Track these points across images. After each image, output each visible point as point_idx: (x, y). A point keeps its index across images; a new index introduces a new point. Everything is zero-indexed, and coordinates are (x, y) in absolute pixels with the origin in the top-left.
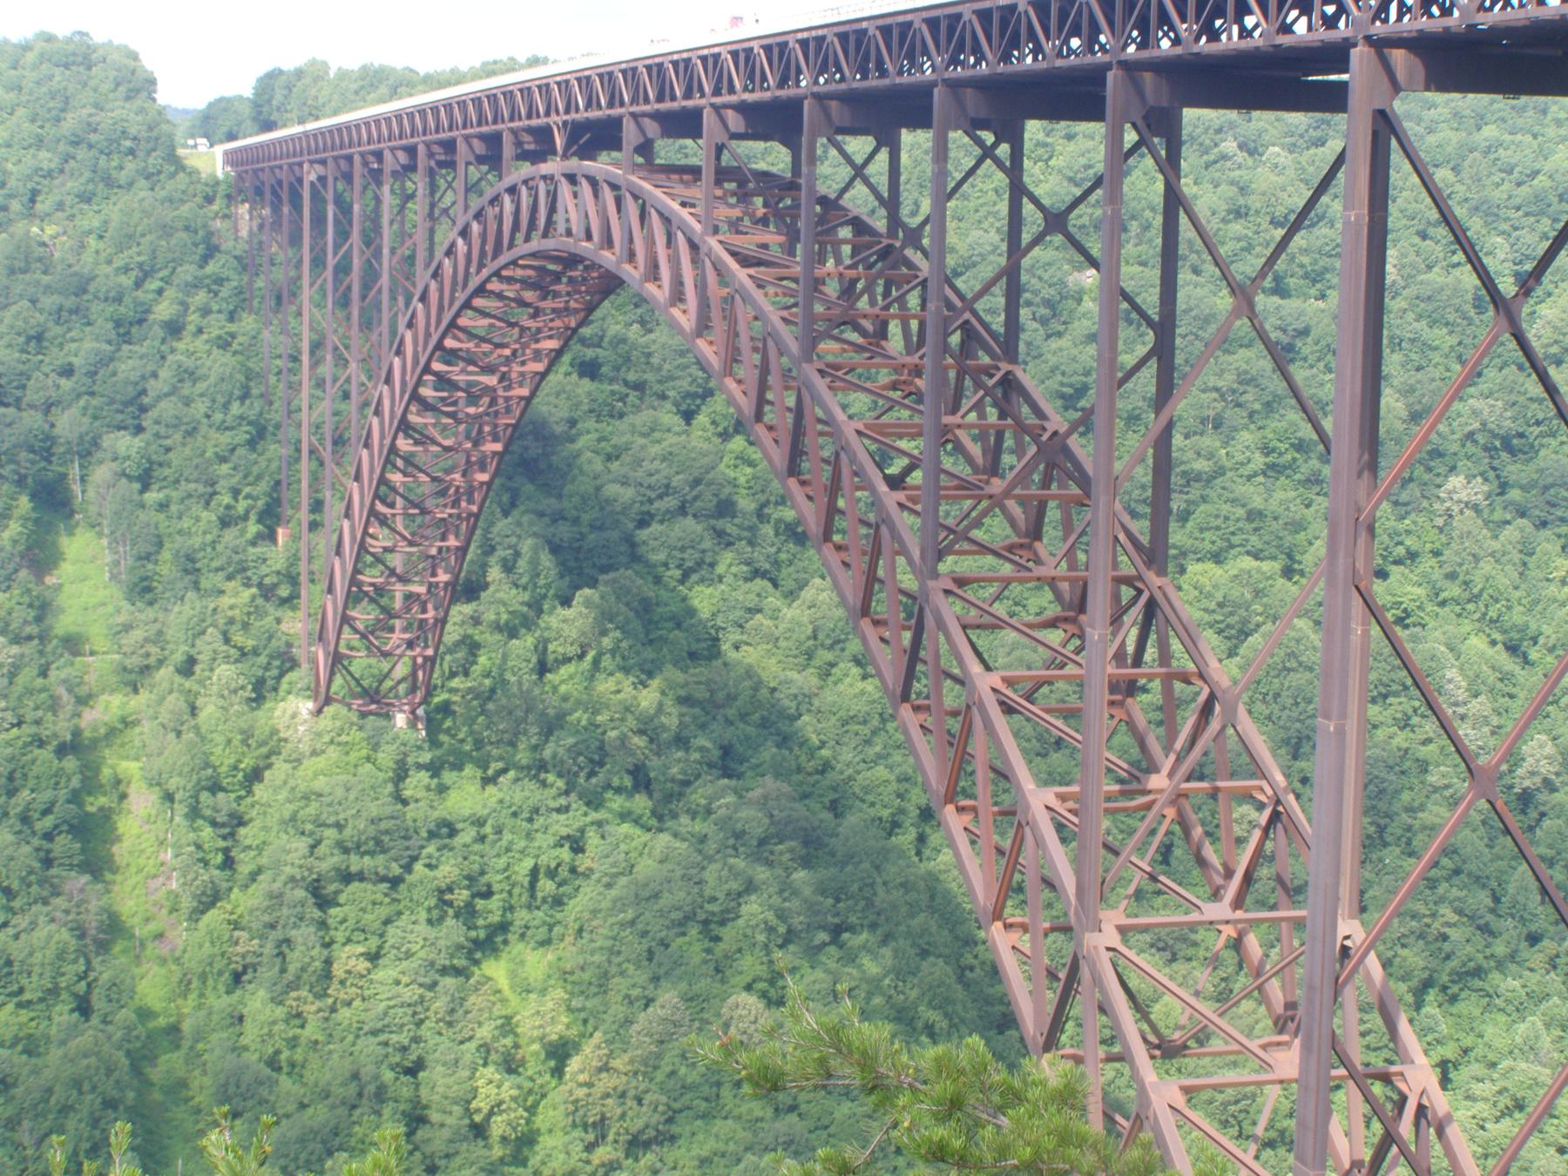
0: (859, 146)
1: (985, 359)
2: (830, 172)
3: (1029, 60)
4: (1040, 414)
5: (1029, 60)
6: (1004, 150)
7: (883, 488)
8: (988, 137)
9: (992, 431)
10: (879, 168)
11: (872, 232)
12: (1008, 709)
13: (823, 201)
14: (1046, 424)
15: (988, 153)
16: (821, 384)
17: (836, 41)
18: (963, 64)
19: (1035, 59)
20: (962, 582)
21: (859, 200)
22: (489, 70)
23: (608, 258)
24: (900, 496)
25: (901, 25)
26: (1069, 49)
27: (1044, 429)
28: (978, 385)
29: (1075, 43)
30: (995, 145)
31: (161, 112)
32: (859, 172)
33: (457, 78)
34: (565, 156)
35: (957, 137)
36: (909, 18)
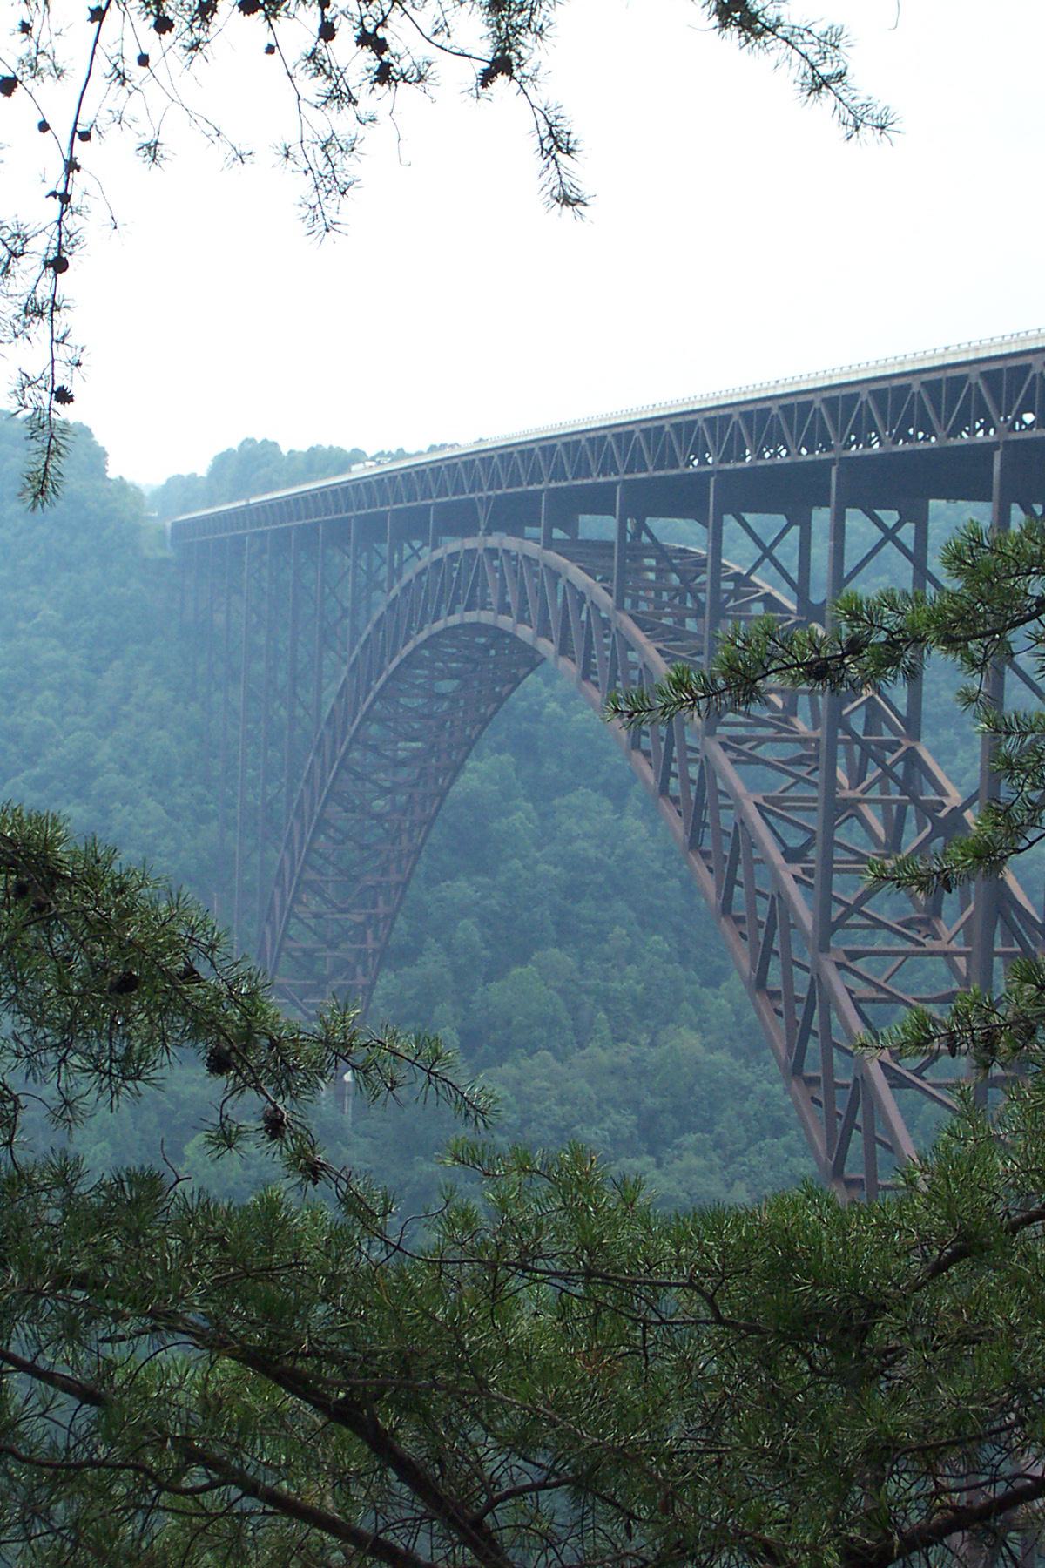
0: (767, 523)
1: (888, 736)
2: (738, 555)
3: (981, 434)
4: (941, 791)
5: (981, 434)
6: (907, 533)
7: (778, 859)
8: (890, 517)
9: (894, 807)
10: (788, 552)
11: (784, 609)
12: (897, 1081)
13: (737, 577)
14: (945, 801)
15: (890, 534)
16: (722, 759)
17: (780, 413)
18: (908, 438)
19: (986, 433)
20: (854, 955)
21: (764, 582)
22: (432, 449)
23: (525, 633)
24: (797, 869)
25: (688, 423)
26: (1022, 422)
27: (944, 806)
28: (881, 763)
29: (1029, 418)
30: (898, 526)
31: (122, 486)
32: (767, 553)
33: (401, 455)
34: (489, 532)
35: (855, 520)
36: (810, 397)
